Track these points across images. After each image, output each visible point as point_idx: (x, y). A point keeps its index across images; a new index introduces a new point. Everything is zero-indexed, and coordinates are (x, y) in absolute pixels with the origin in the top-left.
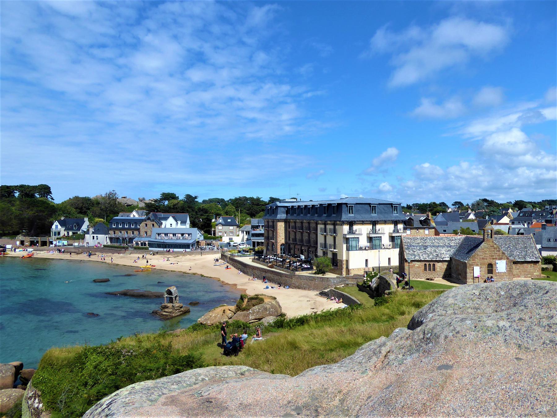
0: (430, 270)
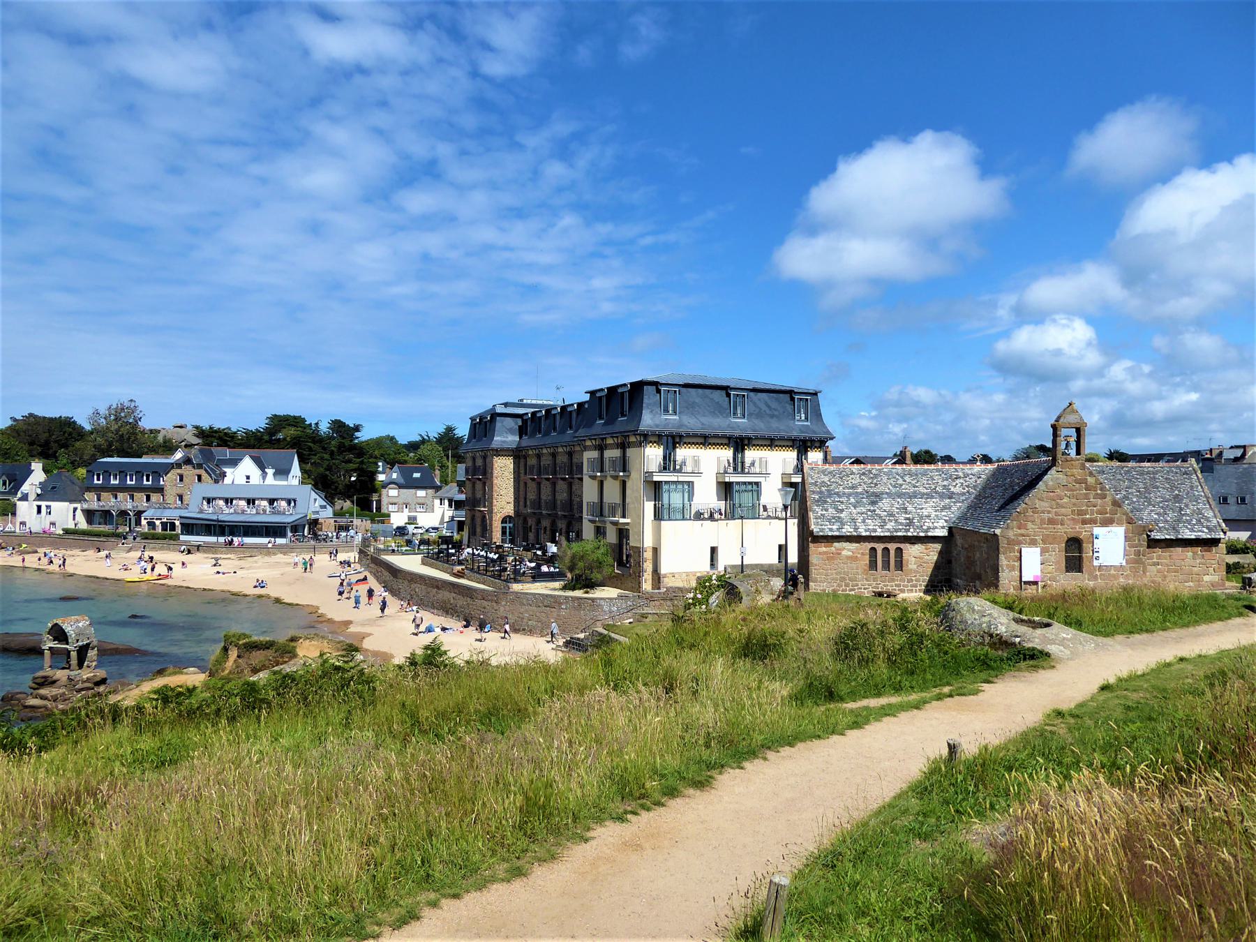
0: (886, 566)
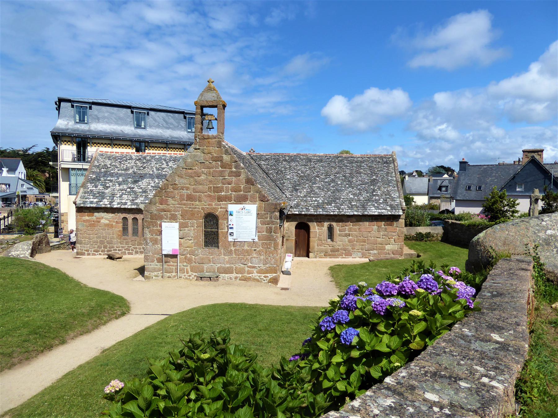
0: (135, 232)
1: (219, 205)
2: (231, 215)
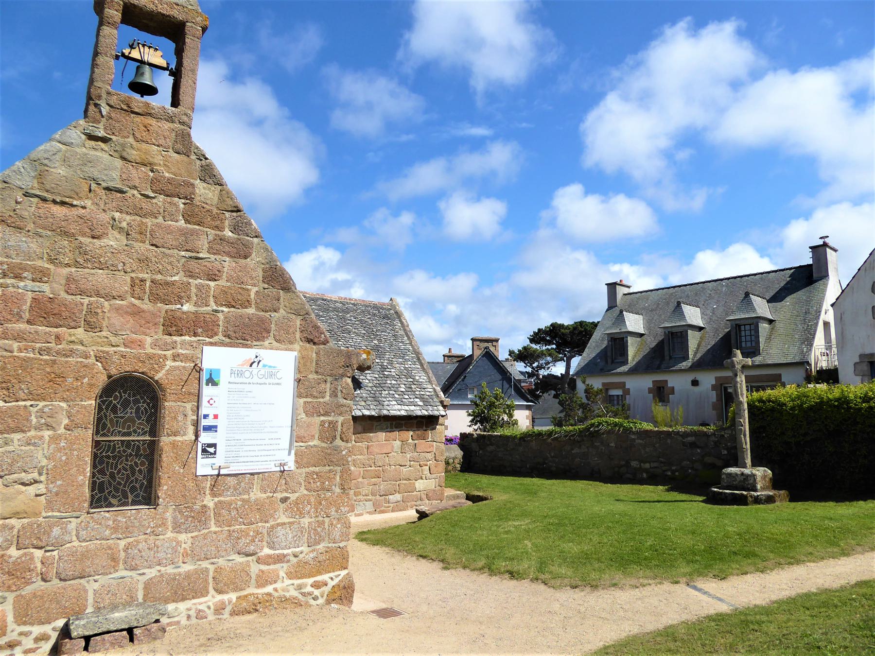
1: (165, 347)
2: (212, 382)
